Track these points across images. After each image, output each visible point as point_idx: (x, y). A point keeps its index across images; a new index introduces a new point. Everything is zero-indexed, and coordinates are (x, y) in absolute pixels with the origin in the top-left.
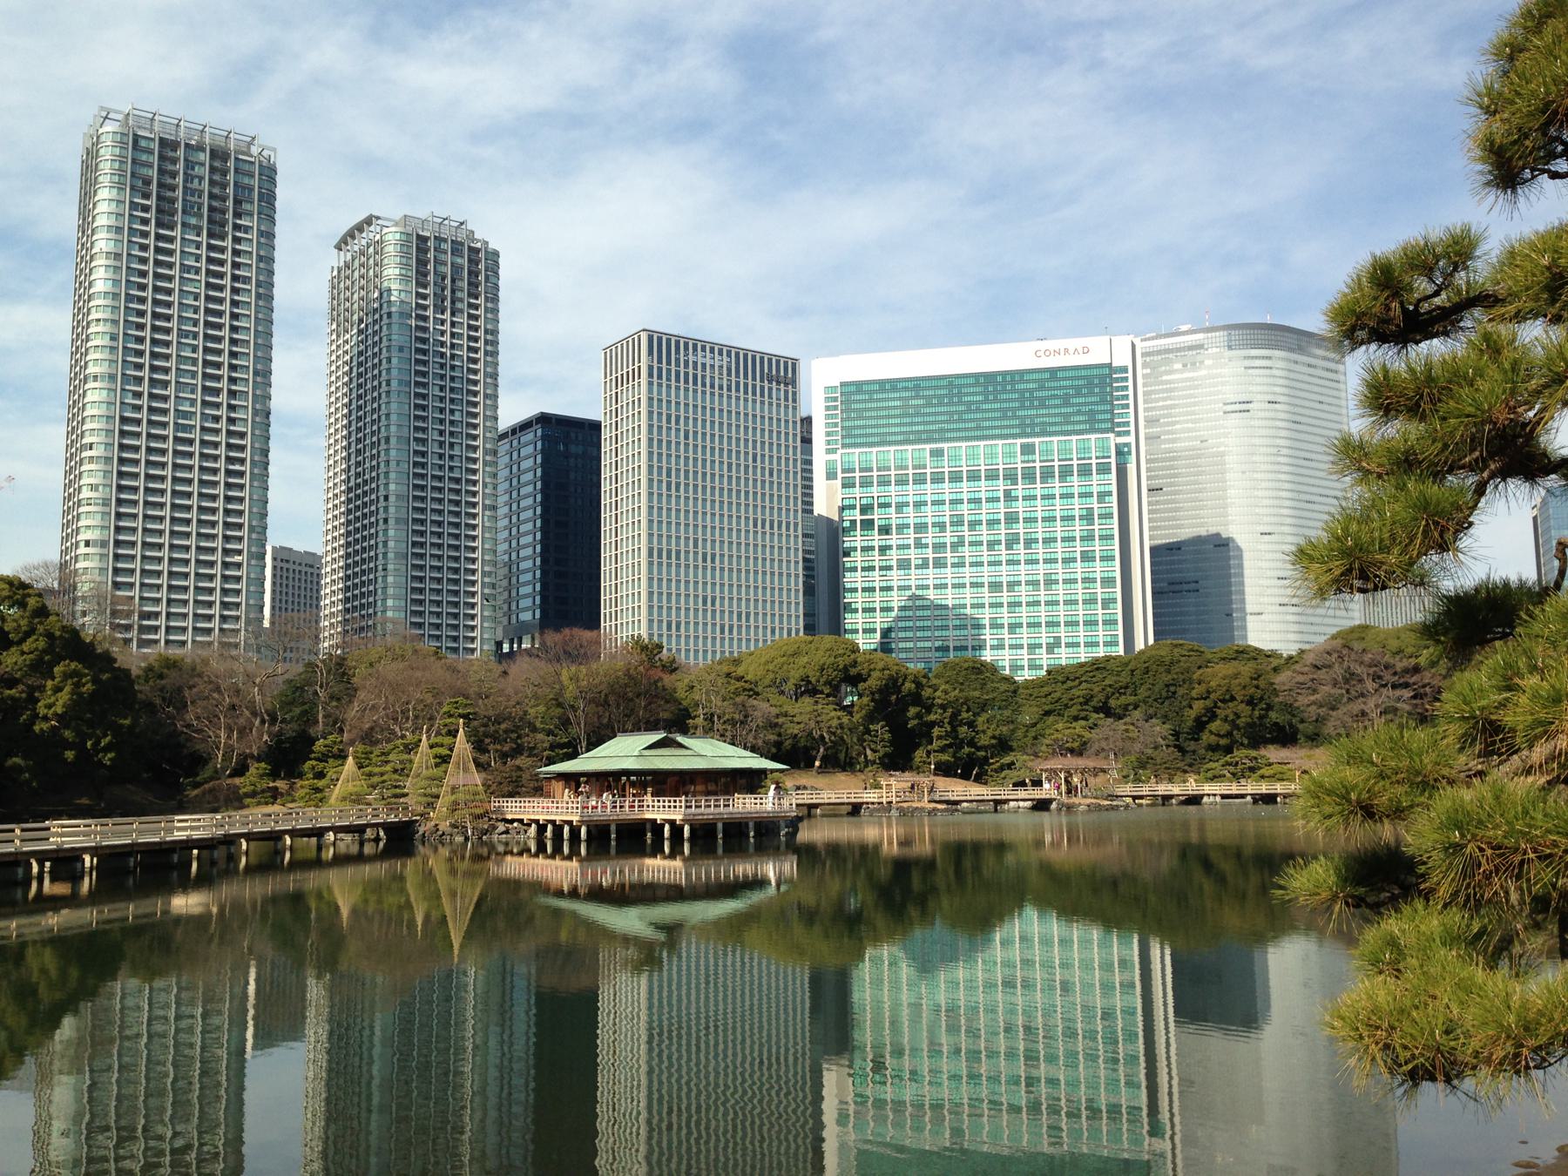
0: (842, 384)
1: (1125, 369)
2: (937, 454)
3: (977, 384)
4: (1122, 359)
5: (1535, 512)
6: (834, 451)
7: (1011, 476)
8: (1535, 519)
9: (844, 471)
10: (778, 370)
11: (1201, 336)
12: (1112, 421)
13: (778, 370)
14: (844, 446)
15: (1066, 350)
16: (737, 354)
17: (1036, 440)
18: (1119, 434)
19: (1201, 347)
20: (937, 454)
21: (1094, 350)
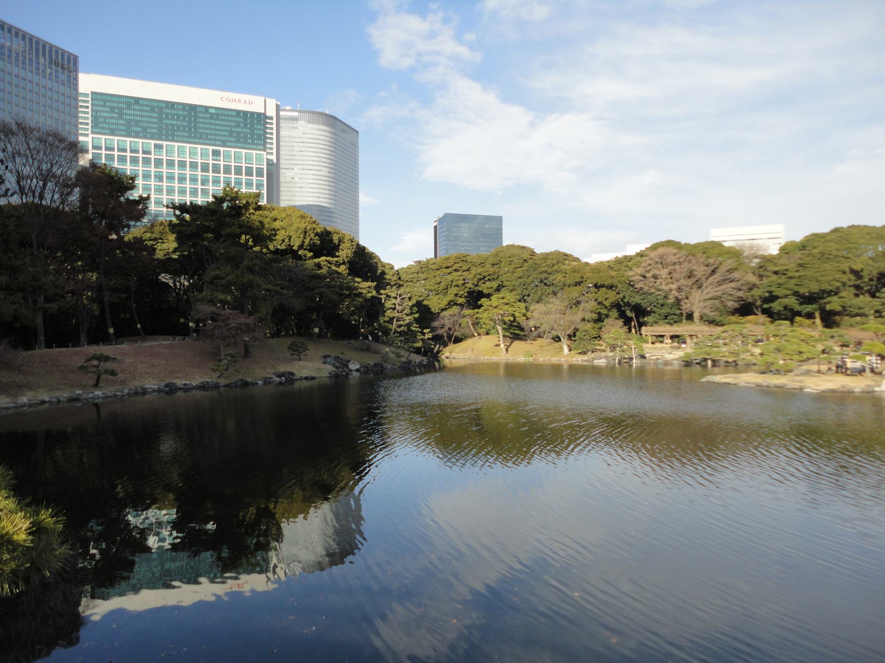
0: (92, 93)
1: (271, 118)
2: (158, 147)
3: (184, 109)
4: (271, 112)
5: (436, 224)
6: (87, 135)
7: (205, 168)
8: (435, 227)
9: (94, 148)
10: (63, 59)
11: (296, 114)
12: (265, 147)
13: (63, 59)
14: (92, 132)
15: (239, 101)
16: (31, 40)
17: (222, 149)
18: (267, 153)
19: (295, 119)
20: (158, 147)
21: (253, 103)
